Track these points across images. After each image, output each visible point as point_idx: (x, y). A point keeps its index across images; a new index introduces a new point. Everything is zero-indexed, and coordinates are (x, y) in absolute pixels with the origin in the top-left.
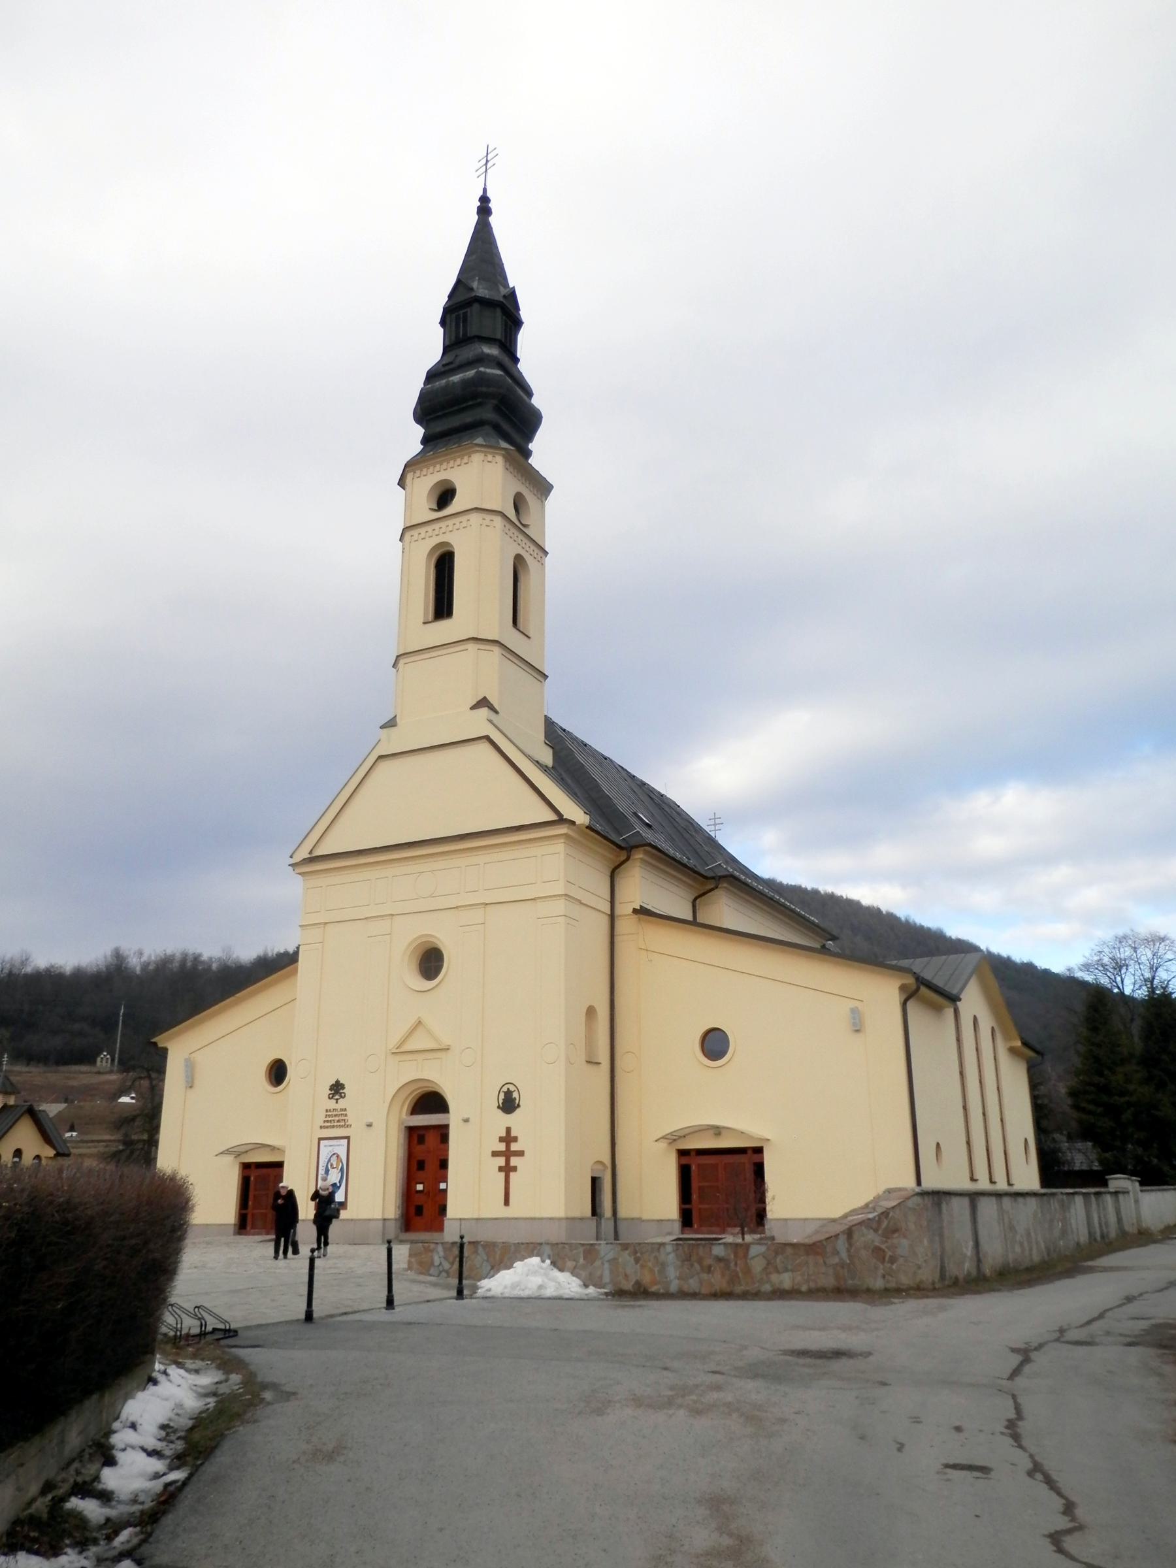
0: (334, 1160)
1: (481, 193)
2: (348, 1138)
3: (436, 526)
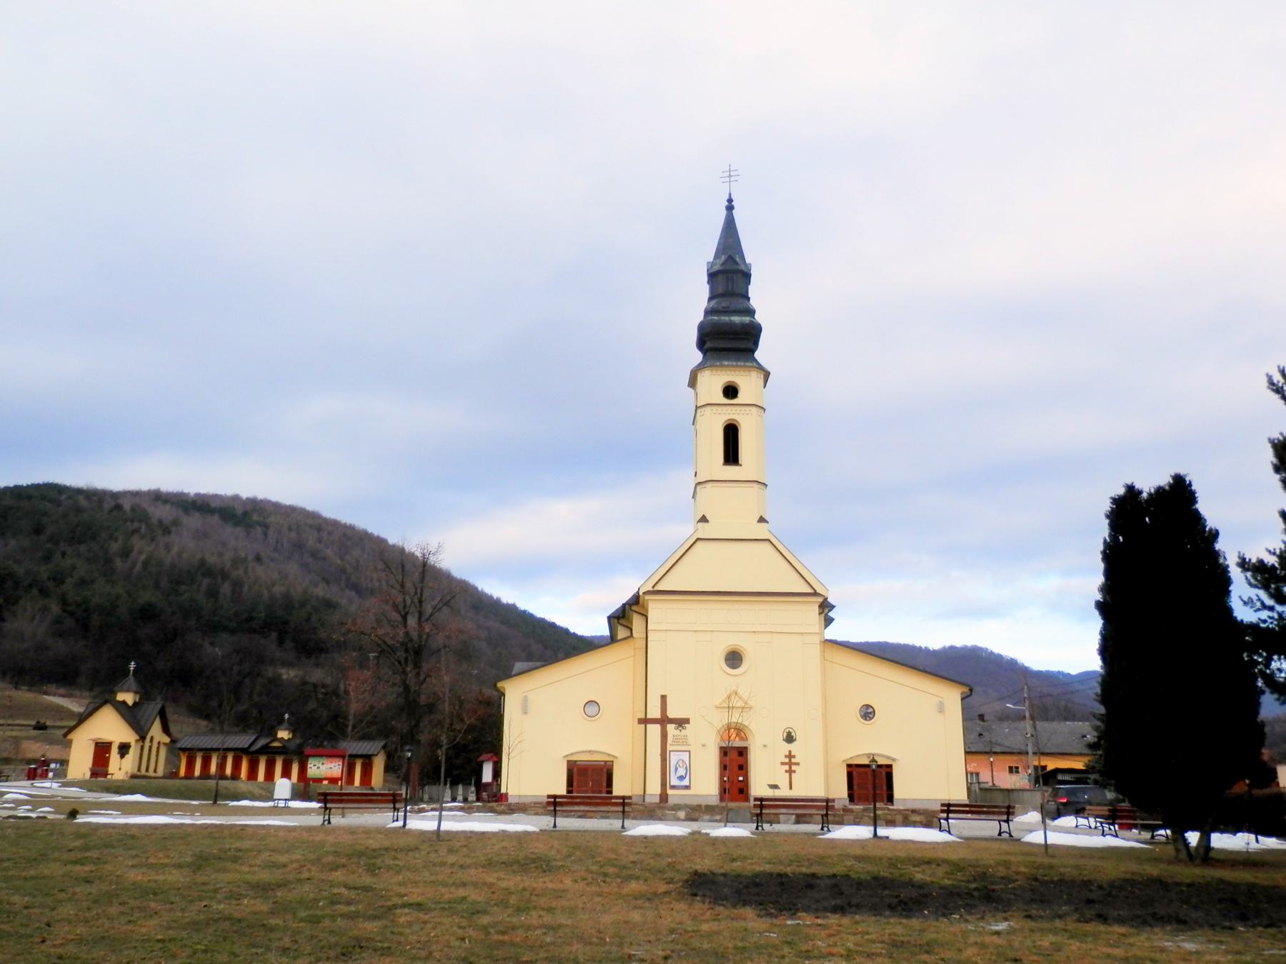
0: (680, 763)
2: (689, 752)
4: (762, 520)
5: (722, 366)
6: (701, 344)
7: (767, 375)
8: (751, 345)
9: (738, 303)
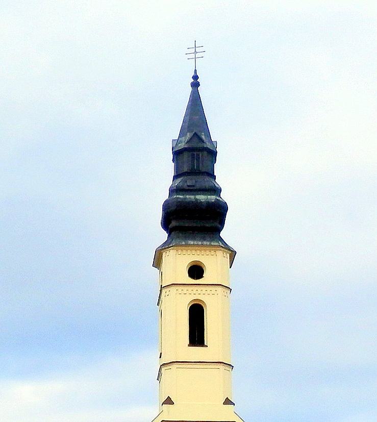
1: (193, 74)
3: (190, 288)
4: (228, 402)
5: (187, 245)
6: (166, 224)
7: (233, 254)
8: (217, 225)
9: (204, 182)
